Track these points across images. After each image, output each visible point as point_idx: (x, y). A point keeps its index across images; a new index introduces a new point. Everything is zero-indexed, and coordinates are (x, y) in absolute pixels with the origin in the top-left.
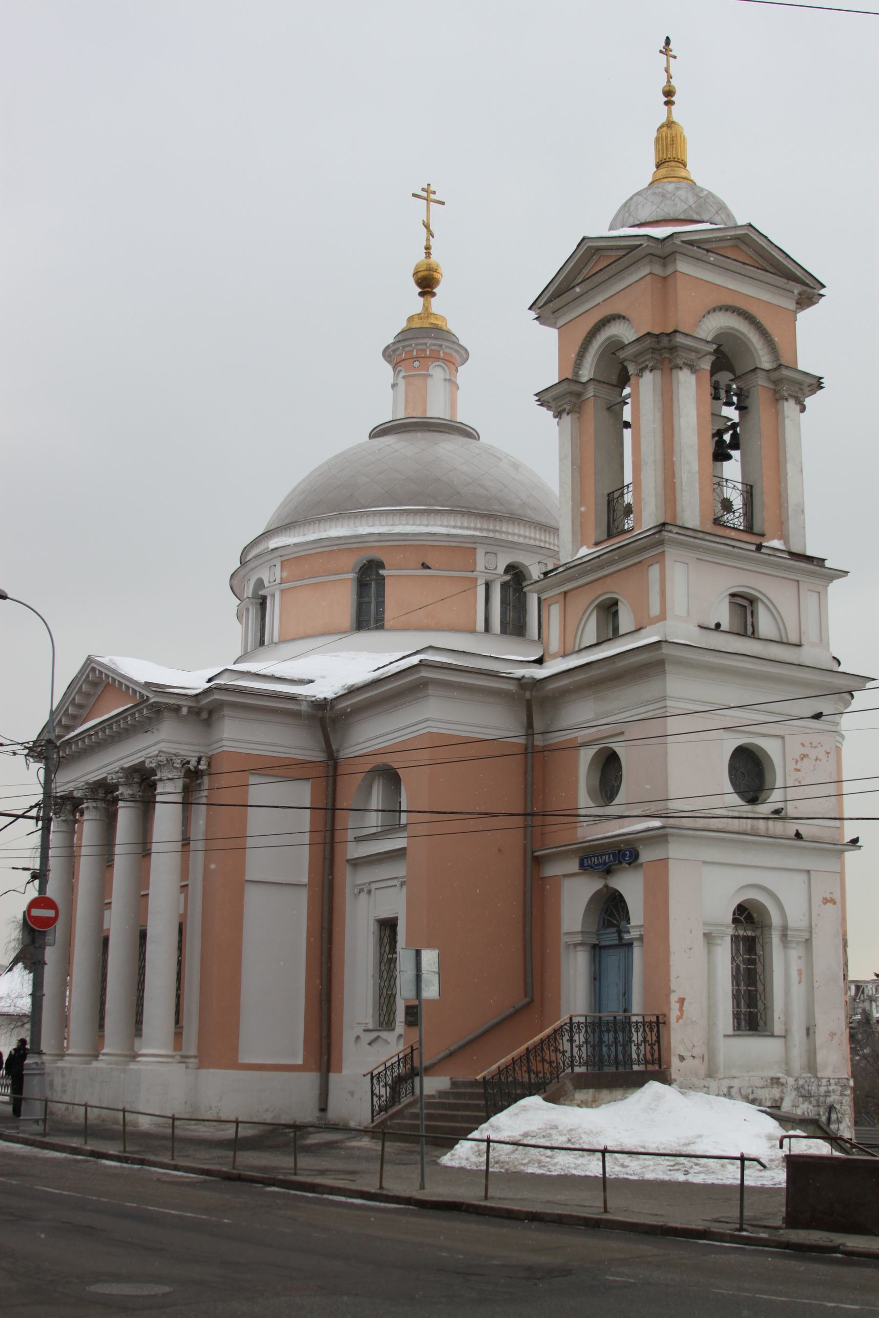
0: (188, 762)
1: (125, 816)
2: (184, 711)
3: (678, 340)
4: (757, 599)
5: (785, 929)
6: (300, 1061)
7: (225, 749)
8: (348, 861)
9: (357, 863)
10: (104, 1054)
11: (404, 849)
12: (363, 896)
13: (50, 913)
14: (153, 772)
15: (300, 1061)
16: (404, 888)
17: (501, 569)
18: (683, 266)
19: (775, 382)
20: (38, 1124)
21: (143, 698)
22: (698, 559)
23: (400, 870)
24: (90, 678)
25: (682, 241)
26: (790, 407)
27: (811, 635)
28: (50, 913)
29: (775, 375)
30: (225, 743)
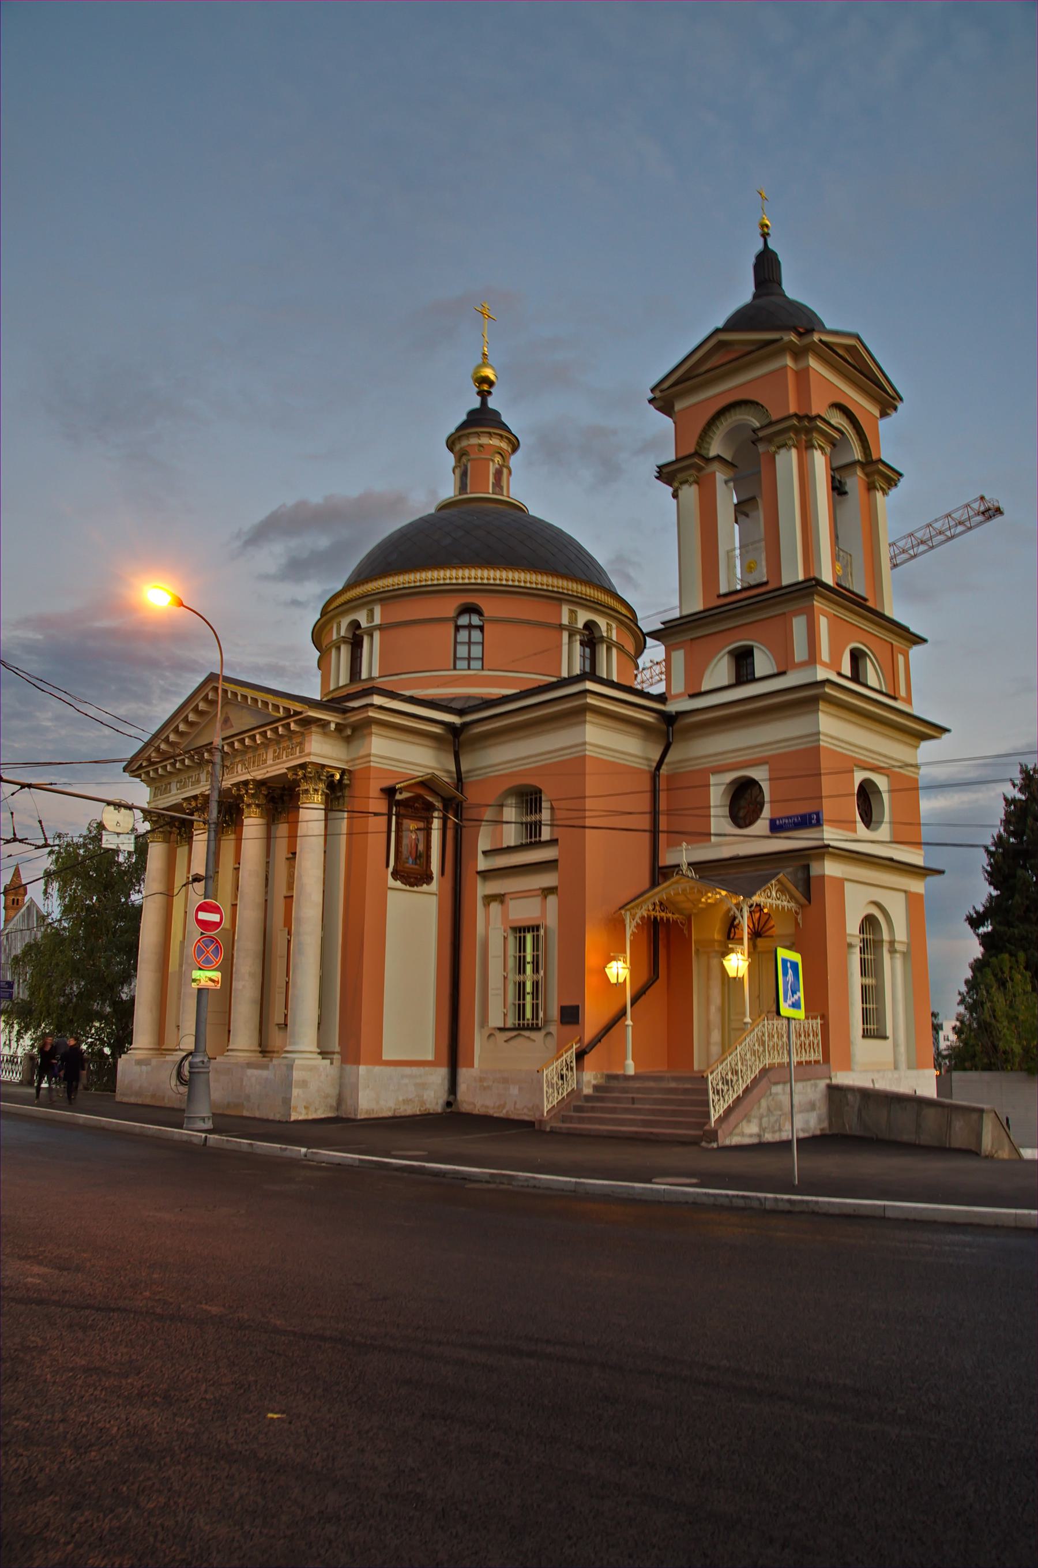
0: (333, 776)
1: (253, 825)
2: (333, 726)
3: (818, 423)
4: (866, 654)
5: (892, 943)
6: (430, 1057)
7: (372, 764)
8: (478, 873)
9: (486, 875)
10: (232, 1050)
11: (556, 861)
12: (495, 907)
13: (203, 916)
14: (296, 783)
15: (430, 1057)
16: (552, 900)
17: (580, 625)
18: (813, 363)
19: (867, 475)
20: (204, 1122)
21: (290, 711)
22: (834, 615)
23: (548, 880)
24: (210, 698)
25: (820, 341)
26: (879, 495)
27: (903, 693)
28: (203, 916)
29: (869, 469)
30: (372, 759)
